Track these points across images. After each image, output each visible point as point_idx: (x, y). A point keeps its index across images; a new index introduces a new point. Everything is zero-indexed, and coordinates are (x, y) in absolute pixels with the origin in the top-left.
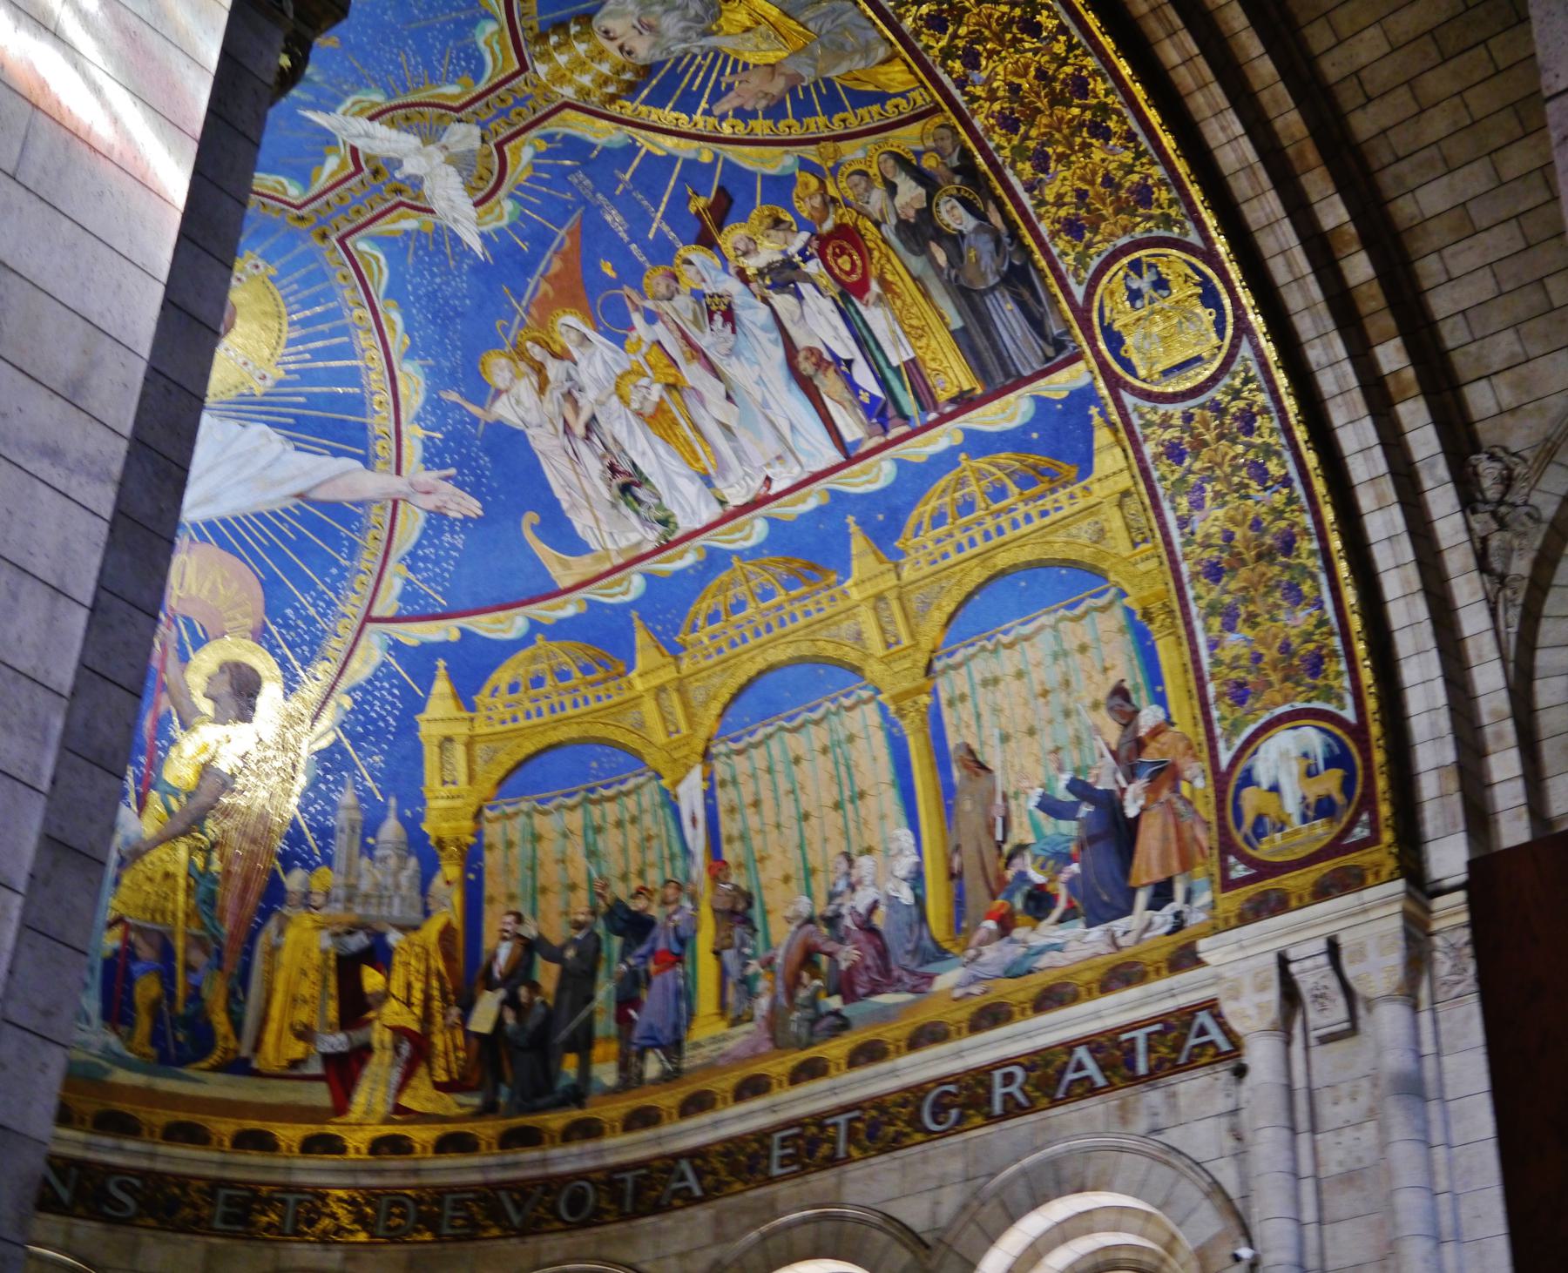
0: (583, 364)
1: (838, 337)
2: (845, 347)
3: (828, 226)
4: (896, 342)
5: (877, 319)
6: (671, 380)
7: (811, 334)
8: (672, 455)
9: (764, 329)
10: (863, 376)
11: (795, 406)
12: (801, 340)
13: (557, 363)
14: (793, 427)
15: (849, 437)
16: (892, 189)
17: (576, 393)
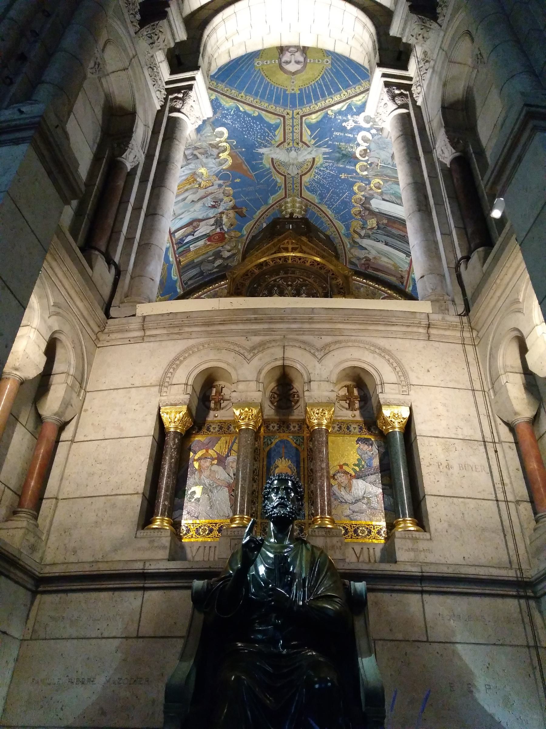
0: (214, 161)
1: (200, 233)
2: (197, 234)
3: (226, 236)
4: (195, 247)
5: (201, 243)
6: (202, 186)
7: (202, 226)
8: (181, 181)
9: (207, 214)
10: (190, 238)
11: (186, 219)
12: (202, 224)
13: (217, 153)
14: (181, 218)
15: (176, 234)
16: (229, 251)
17: (206, 155)
